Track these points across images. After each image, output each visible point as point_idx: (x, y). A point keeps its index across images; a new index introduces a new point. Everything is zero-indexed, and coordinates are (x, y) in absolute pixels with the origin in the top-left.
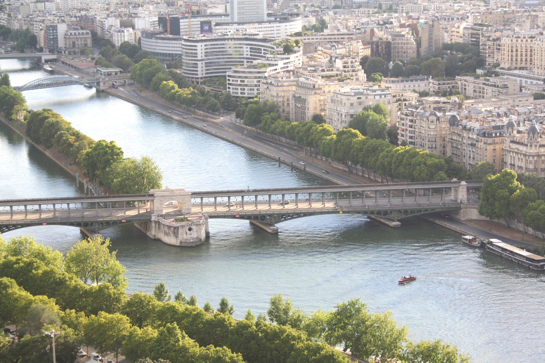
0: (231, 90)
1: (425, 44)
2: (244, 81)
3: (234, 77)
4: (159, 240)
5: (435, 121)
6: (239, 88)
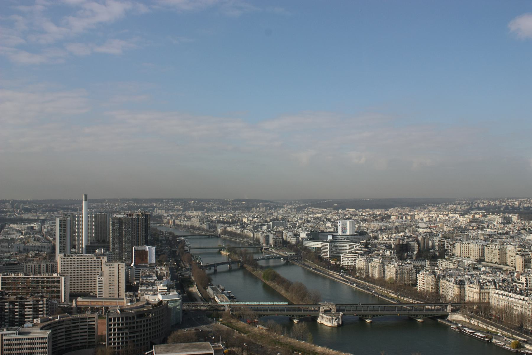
0: (343, 263)
1: (422, 245)
2: (347, 259)
3: (344, 257)
4: (322, 324)
6: (347, 262)
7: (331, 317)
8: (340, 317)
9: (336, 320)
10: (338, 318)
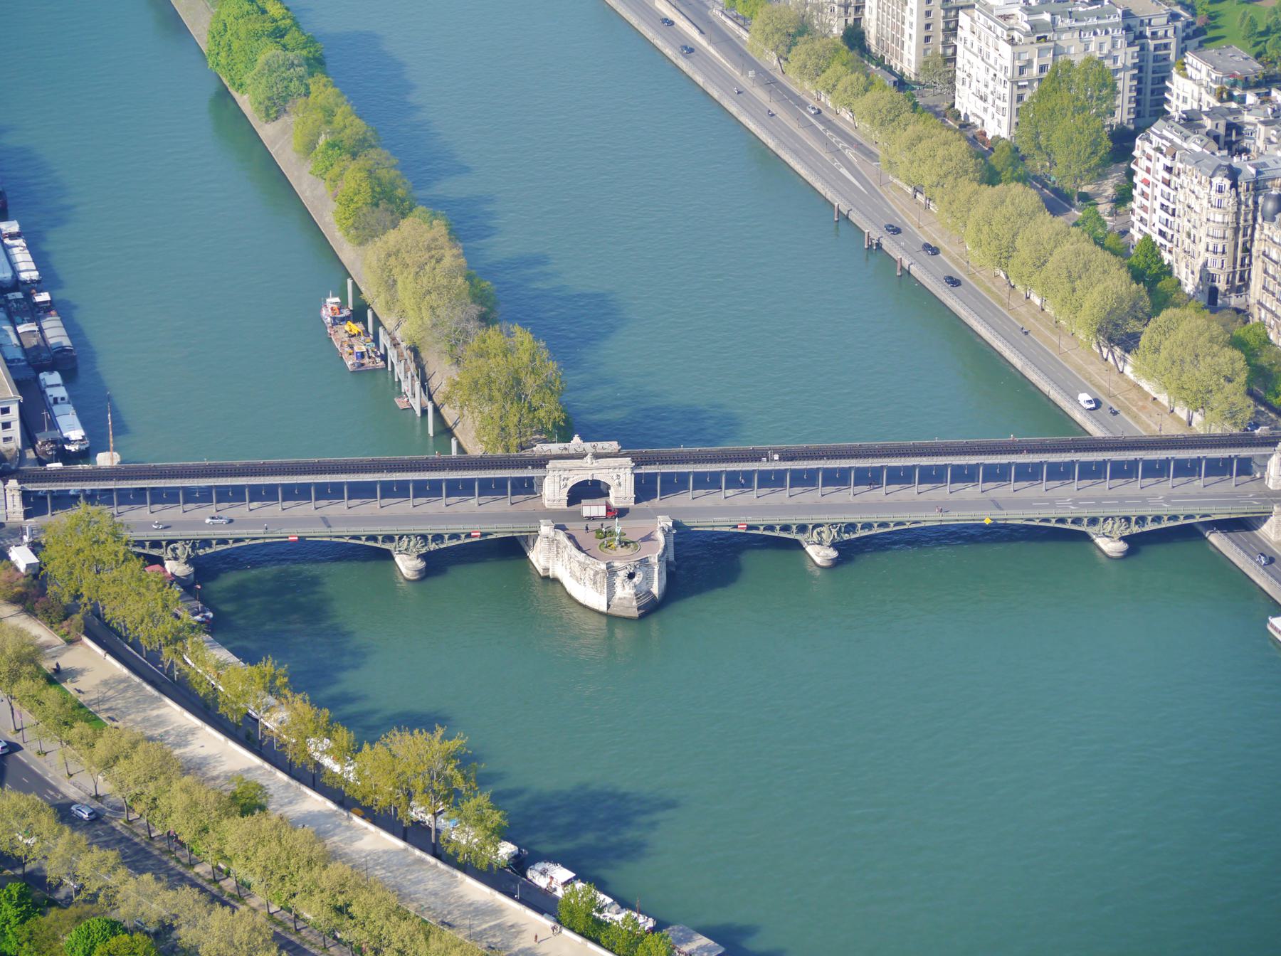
5: (1228, 187)
7: (604, 566)
8: (654, 559)
9: (631, 576)
10: (644, 562)
